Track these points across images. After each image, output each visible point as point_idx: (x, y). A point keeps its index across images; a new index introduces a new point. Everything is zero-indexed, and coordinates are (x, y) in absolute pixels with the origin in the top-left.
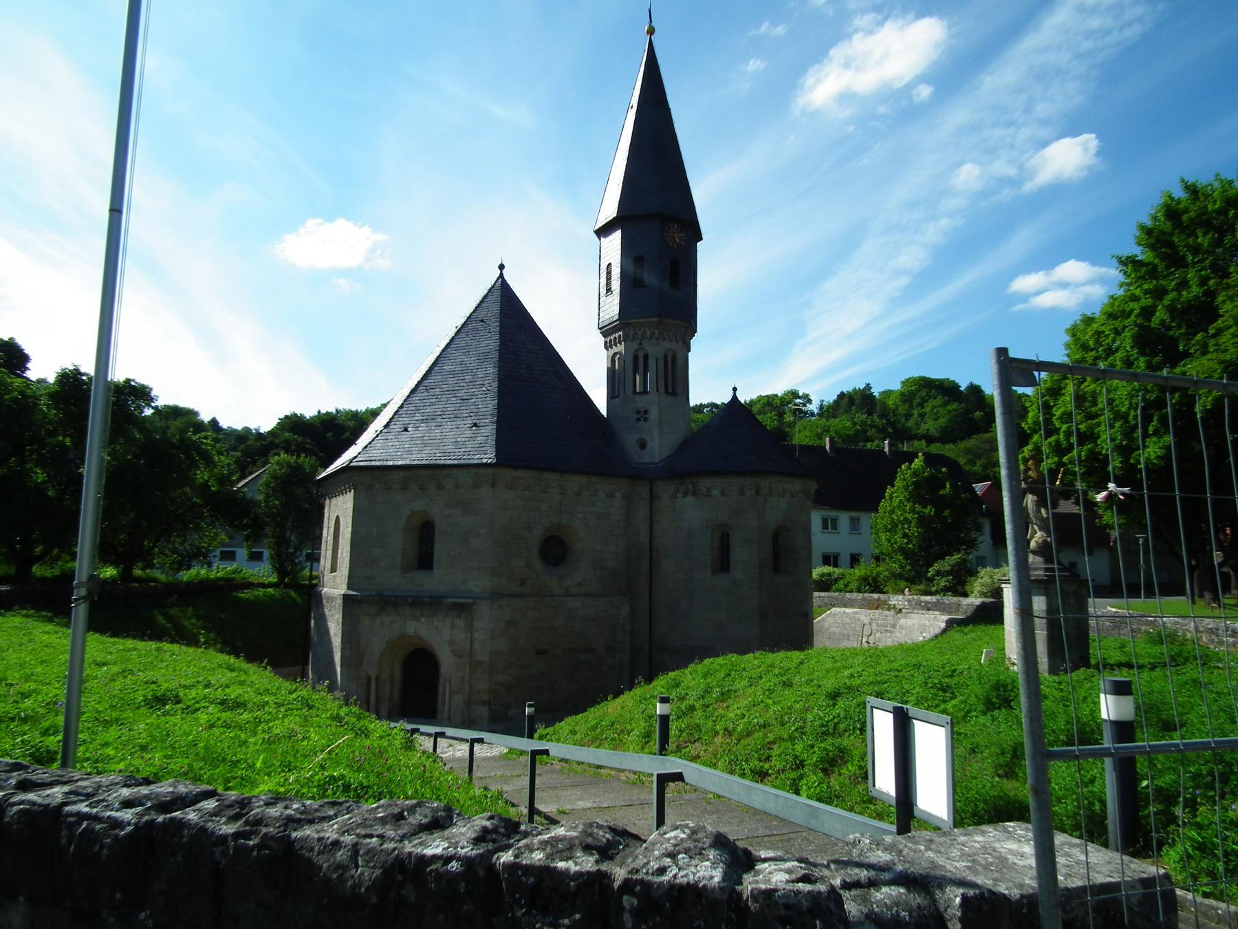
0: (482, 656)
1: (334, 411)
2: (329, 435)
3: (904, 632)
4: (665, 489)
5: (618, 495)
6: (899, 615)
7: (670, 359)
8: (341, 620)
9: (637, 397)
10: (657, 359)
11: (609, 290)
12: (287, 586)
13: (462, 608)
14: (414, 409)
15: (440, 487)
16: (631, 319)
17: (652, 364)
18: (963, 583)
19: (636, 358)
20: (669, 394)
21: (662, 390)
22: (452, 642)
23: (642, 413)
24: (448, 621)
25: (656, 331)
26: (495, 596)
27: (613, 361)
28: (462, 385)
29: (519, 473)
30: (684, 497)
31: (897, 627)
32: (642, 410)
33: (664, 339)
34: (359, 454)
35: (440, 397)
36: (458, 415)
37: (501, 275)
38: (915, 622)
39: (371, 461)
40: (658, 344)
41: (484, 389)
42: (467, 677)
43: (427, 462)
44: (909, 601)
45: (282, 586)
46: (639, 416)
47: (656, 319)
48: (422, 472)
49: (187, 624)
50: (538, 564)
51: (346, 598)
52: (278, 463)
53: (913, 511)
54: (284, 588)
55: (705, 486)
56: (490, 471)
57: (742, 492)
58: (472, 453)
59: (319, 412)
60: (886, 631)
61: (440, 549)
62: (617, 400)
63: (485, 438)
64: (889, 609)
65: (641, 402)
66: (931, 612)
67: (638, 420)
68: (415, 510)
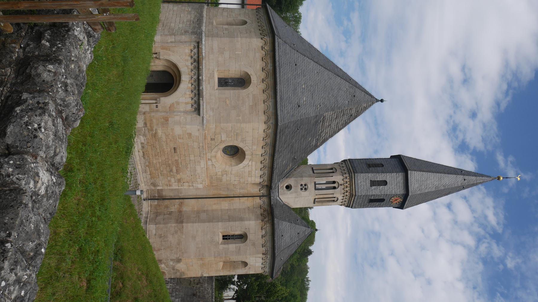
9: (313, 184)
17: (331, 191)
19: (334, 182)
21: (317, 197)
22: (178, 103)
30: (261, 214)
32: (306, 187)
33: (343, 197)
37: (377, 101)
39: (278, 46)
46: (303, 186)
50: (223, 146)
62: (311, 172)
65: (311, 186)
67: (302, 185)
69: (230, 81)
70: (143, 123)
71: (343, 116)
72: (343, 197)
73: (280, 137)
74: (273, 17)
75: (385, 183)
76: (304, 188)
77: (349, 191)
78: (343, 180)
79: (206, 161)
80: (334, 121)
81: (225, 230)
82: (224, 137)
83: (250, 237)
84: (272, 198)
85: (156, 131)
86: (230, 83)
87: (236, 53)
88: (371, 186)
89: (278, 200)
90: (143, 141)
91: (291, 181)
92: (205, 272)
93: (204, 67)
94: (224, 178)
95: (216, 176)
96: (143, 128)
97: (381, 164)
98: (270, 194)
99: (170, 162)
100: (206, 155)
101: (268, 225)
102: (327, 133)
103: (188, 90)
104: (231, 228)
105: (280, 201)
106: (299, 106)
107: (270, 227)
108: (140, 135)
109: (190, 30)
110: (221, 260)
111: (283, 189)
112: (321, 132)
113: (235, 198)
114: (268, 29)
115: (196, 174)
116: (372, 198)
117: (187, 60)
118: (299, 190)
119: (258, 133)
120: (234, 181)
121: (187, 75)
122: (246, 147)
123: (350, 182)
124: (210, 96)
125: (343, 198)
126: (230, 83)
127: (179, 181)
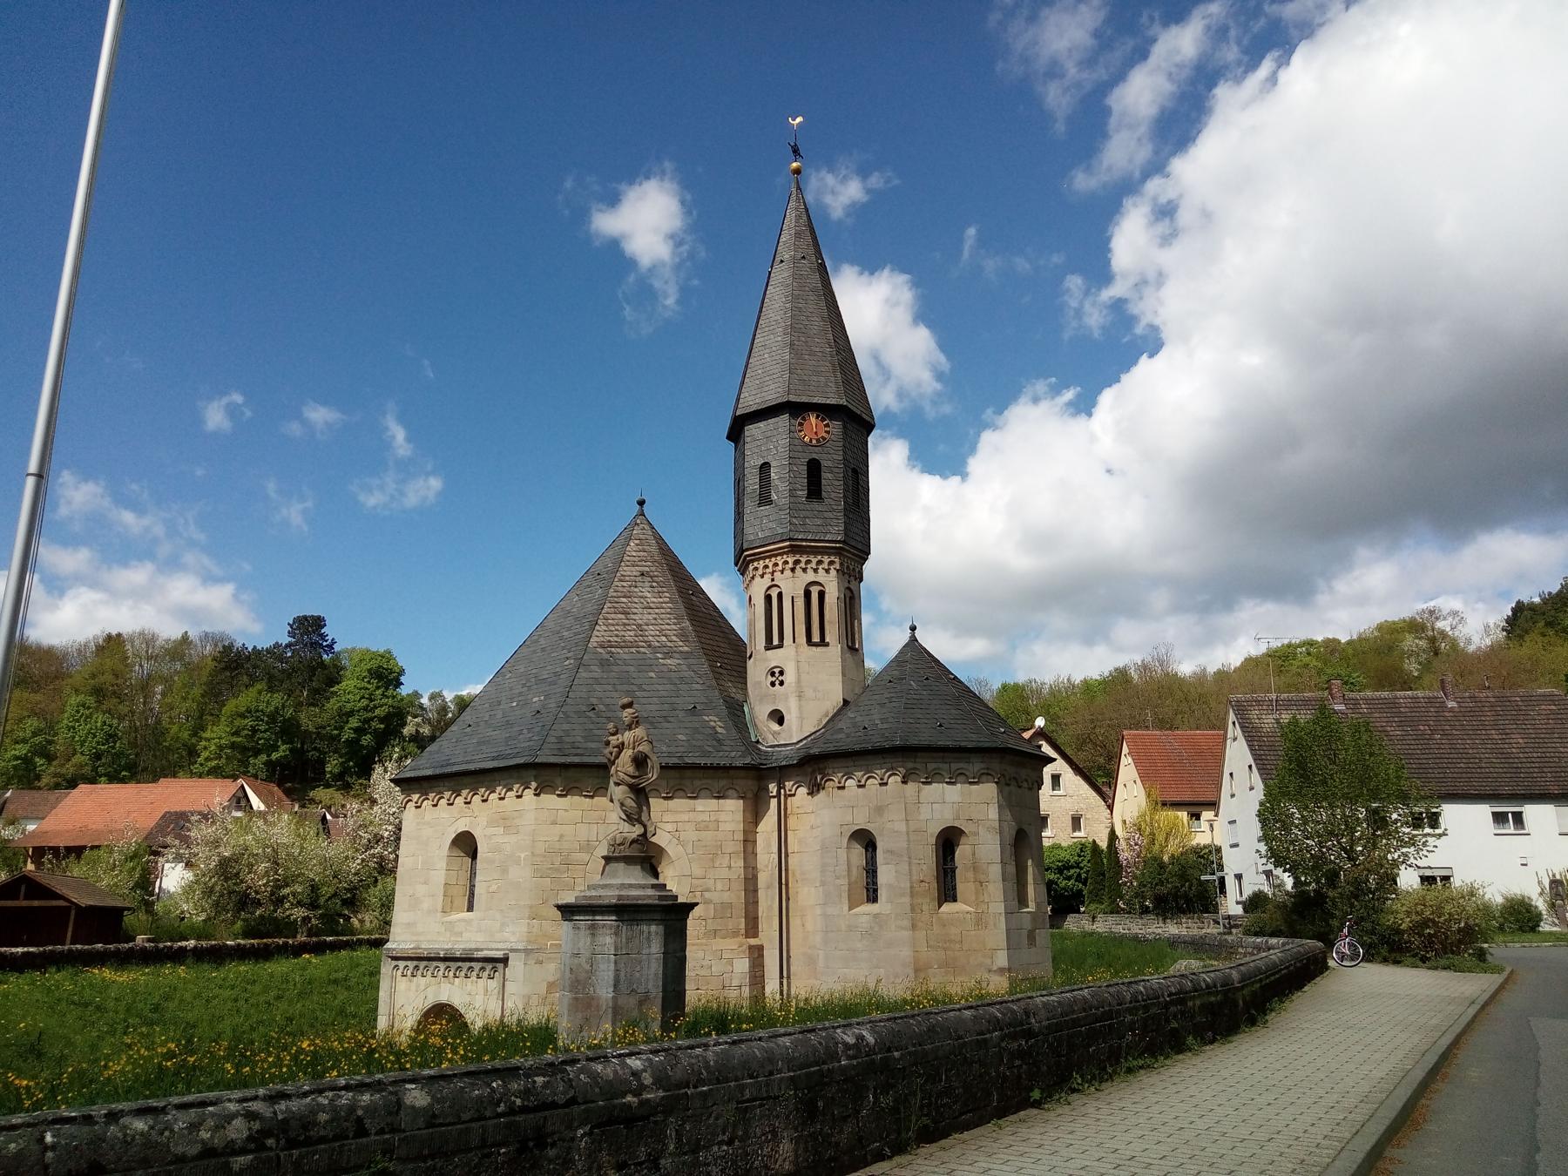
10: (793, 597)
19: (768, 598)
20: (816, 645)
21: (802, 638)
32: (777, 670)
46: (774, 679)
67: (773, 684)
72: (804, 570)
73: (576, 755)
75: (765, 467)
76: (777, 675)
77: (785, 556)
78: (762, 576)
81: (843, 894)
83: (861, 822)
88: (771, 502)
89: (805, 744)
91: (758, 711)
92: (988, 961)
95: (709, 921)
98: (774, 767)
105: (809, 739)
107: (835, 765)
110: (925, 907)
111: (779, 734)
112: (650, 646)
120: (733, 869)
123: (764, 558)
125: (810, 571)
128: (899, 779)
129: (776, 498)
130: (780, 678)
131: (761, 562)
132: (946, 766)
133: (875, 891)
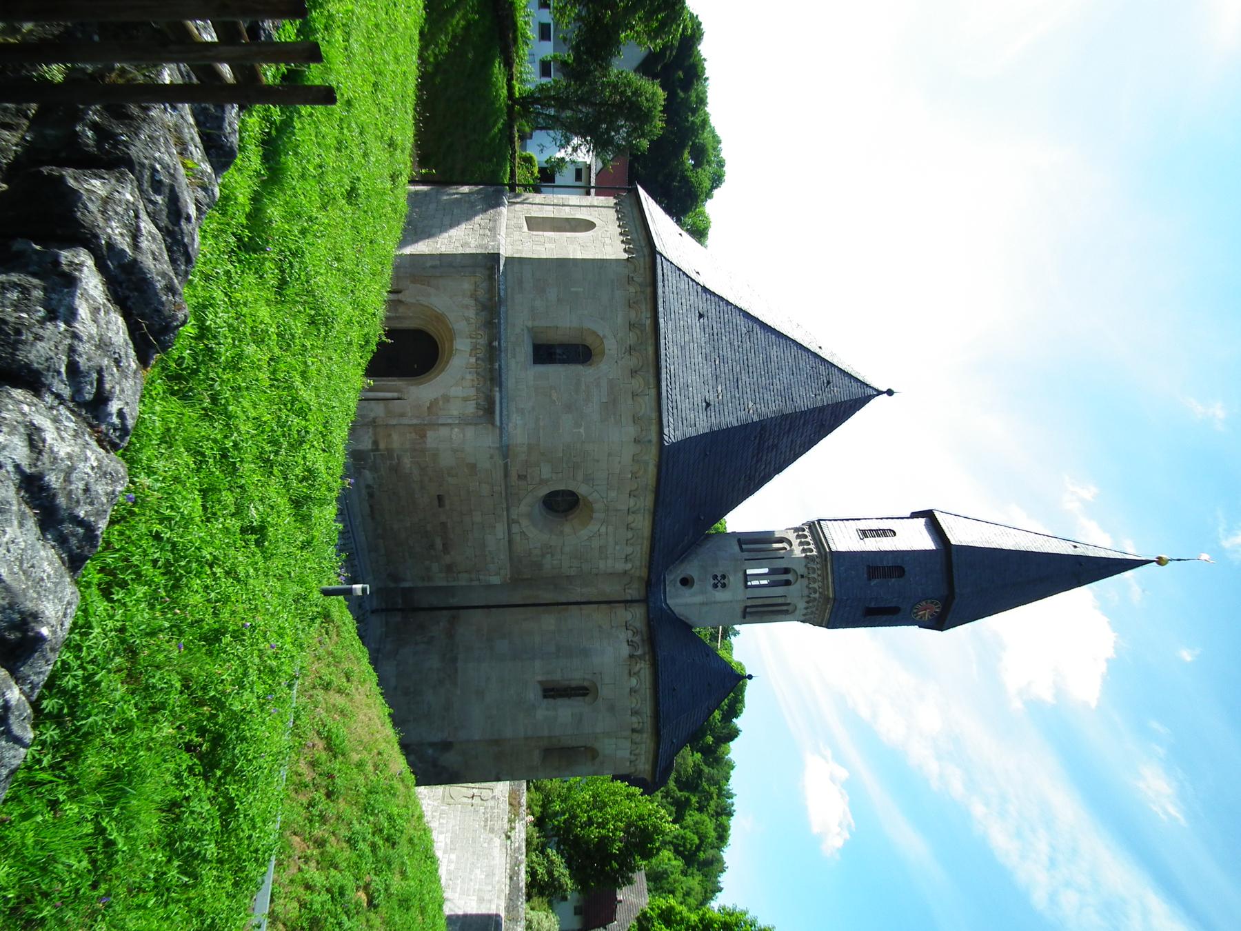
0: (433, 439)
1: (706, 76)
2: (681, 74)
3: (486, 845)
4: (636, 615)
5: (629, 566)
6: (504, 836)
7: (785, 608)
8: (468, 251)
9: (741, 575)
11: (865, 534)
12: (510, 109)
13: (488, 411)
14: (726, 320)
15: (633, 373)
16: (832, 566)
17: (780, 591)
18: (541, 894)
21: (749, 603)
22: (446, 399)
23: (722, 581)
24: (472, 392)
25: (817, 595)
26: (505, 451)
27: (781, 540)
28: (755, 374)
29: (652, 469)
30: (628, 641)
31: (491, 835)
32: (726, 581)
33: (808, 602)
34: (671, 263)
35: (740, 349)
36: (719, 380)
37: (880, 393)
38: (497, 862)
40: (802, 596)
41: (750, 406)
42: (405, 421)
43: (663, 357)
44: (519, 848)
45: (510, 103)
46: (719, 578)
47: (831, 596)
48: (651, 350)
49: (458, 16)
50: (545, 491)
51: (495, 257)
52: (654, 94)
53: (616, 829)
54: (508, 106)
55: (640, 669)
56: (654, 436)
57: (635, 713)
58: (675, 411)
59: (705, 60)
60: (486, 820)
61: (557, 373)
62: (737, 548)
63: (693, 422)
64: (510, 821)
65: (734, 580)
66: (508, 881)
67: (715, 577)
68: (605, 340)
69: (558, 351)
70: (370, 441)
71: (804, 424)
72: (808, 602)
74: (651, 214)
79: (508, 525)
80: (785, 438)
82: (546, 472)
83: (605, 692)
84: (651, 605)
85: (398, 460)
86: (560, 355)
87: (572, 289)
88: (869, 579)
90: (370, 482)
91: (691, 568)
93: (502, 321)
94: (548, 562)
96: (372, 454)
97: (890, 530)
99: (429, 528)
100: (508, 509)
101: (642, 665)
102: (770, 463)
103: (468, 370)
104: (562, 670)
105: (669, 611)
106: (708, 405)
107: (647, 670)
108: (364, 468)
109: (473, 242)
113: (570, 607)
114: (641, 238)
115: (487, 553)
116: (873, 605)
117: (467, 307)
118: (710, 588)
119: (620, 462)
121: (467, 338)
122: (595, 494)
124: (516, 382)
126: (560, 355)
127: (449, 568)
128: (636, 726)
129: (872, 584)
130: (719, 584)
131: (819, 566)
132: (643, 752)
133: (553, 697)
